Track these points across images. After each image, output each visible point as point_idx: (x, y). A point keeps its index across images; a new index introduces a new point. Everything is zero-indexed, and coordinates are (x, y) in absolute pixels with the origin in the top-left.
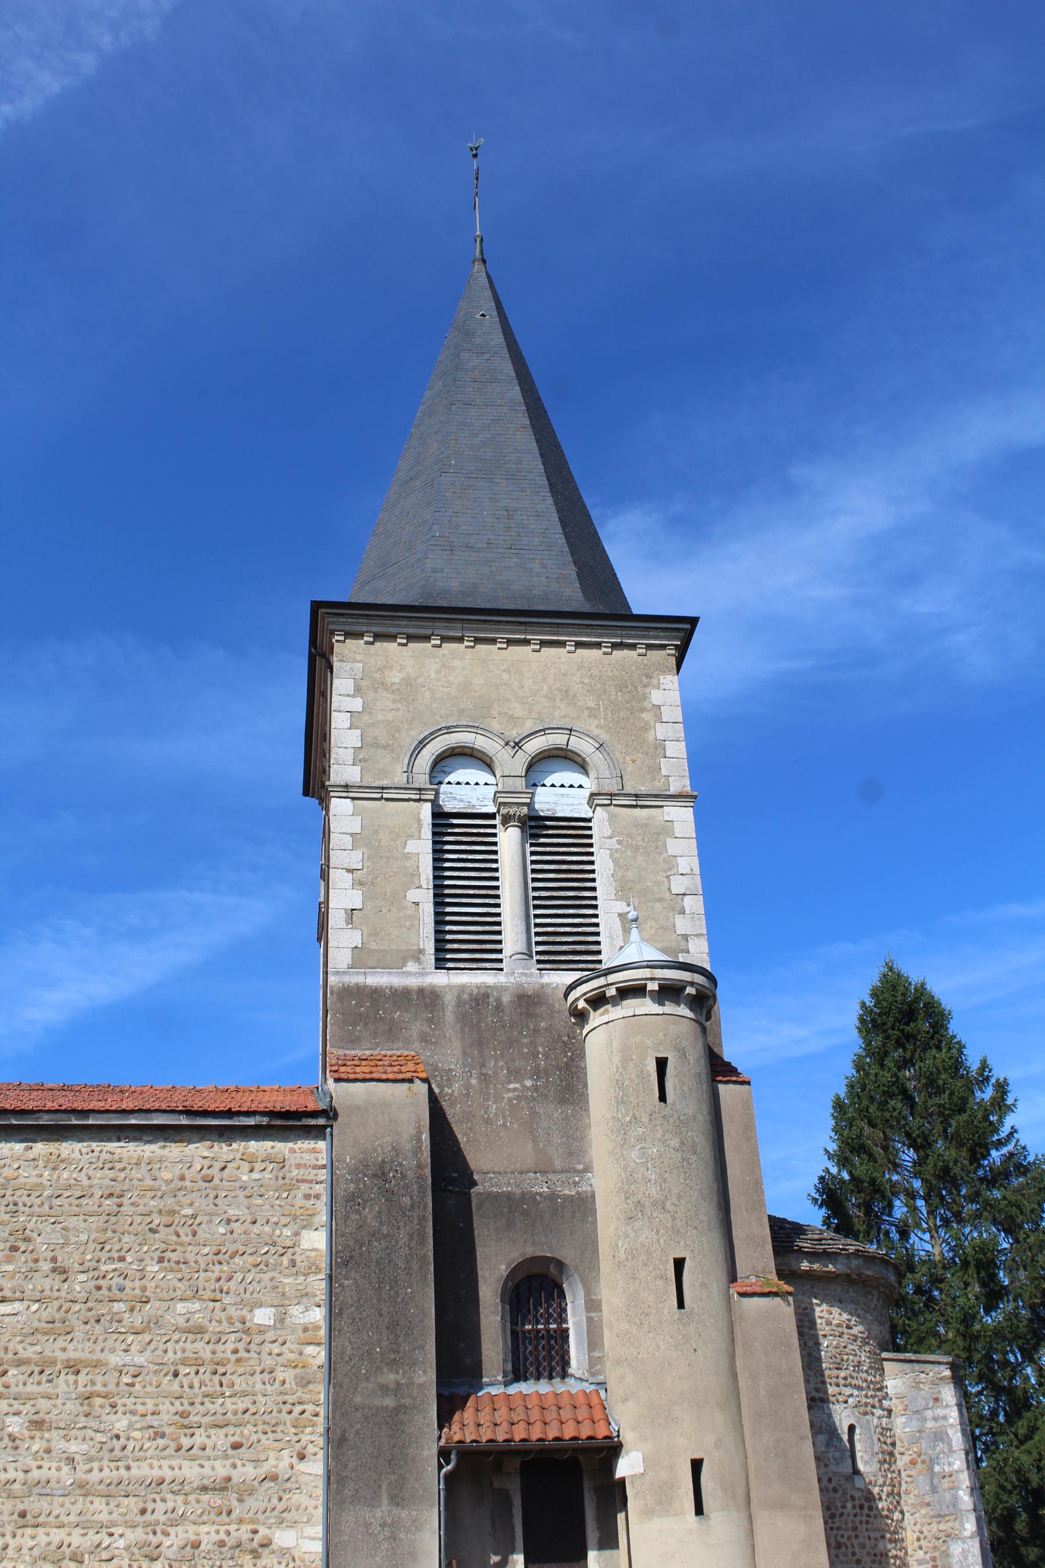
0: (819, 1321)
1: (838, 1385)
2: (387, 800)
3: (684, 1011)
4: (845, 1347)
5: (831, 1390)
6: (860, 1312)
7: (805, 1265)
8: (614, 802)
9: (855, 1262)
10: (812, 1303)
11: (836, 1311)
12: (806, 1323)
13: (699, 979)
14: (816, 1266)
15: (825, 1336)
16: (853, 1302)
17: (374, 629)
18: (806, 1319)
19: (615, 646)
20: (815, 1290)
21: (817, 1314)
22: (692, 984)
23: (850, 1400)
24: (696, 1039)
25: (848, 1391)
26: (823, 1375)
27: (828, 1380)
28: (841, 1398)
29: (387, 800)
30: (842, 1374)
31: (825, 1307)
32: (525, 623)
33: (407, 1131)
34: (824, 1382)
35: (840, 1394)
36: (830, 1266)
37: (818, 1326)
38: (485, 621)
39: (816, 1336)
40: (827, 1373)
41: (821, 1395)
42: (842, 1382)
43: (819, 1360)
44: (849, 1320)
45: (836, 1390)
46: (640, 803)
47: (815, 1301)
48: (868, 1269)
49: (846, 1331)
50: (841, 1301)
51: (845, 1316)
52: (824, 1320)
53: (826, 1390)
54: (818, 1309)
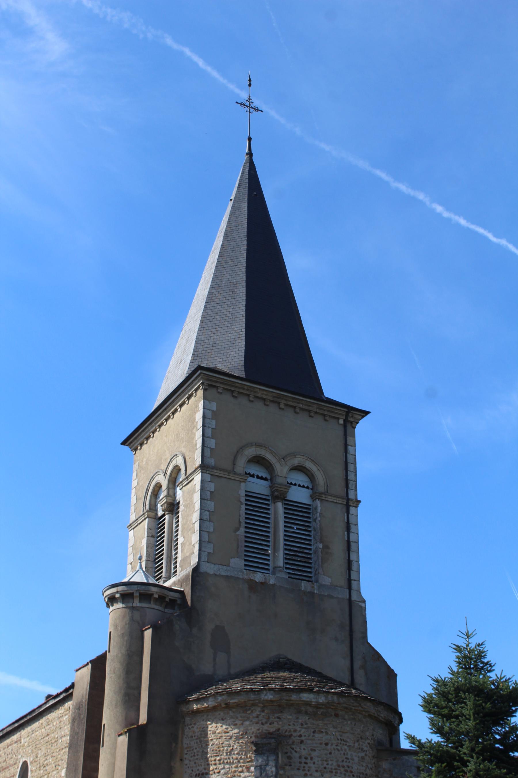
0: (209, 733)
1: (215, 764)
2: (140, 523)
3: (120, 605)
4: (222, 743)
5: (211, 768)
6: (239, 722)
7: (195, 707)
8: (183, 485)
9: (220, 698)
10: (206, 724)
11: (219, 725)
12: (203, 735)
13: (120, 588)
14: (199, 706)
15: (212, 740)
16: (232, 718)
17: (139, 442)
18: (203, 733)
19: (189, 398)
20: (209, 717)
21: (209, 729)
22: (117, 592)
23: (222, 771)
24: (124, 617)
25: (221, 767)
26: (208, 760)
27: (210, 763)
28: (216, 771)
29: (140, 523)
30: (218, 758)
31: (214, 725)
32: (165, 409)
33: (85, 686)
34: (208, 765)
35: (216, 769)
36: (205, 704)
37: (209, 736)
38: (158, 416)
39: (207, 741)
40: (210, 759)
41: (206, 771)
42: (218, 762)
43: (207, 753)
44: (227, 729)
45: (215, 767)
46: (189, 480)
47: (209, 723)
48: (231, 700)
49: (224, 734)
50: (223, 720)
51: (224, 727)
52: (211, 732)
53: (209, 768)
54: (210, 726)
